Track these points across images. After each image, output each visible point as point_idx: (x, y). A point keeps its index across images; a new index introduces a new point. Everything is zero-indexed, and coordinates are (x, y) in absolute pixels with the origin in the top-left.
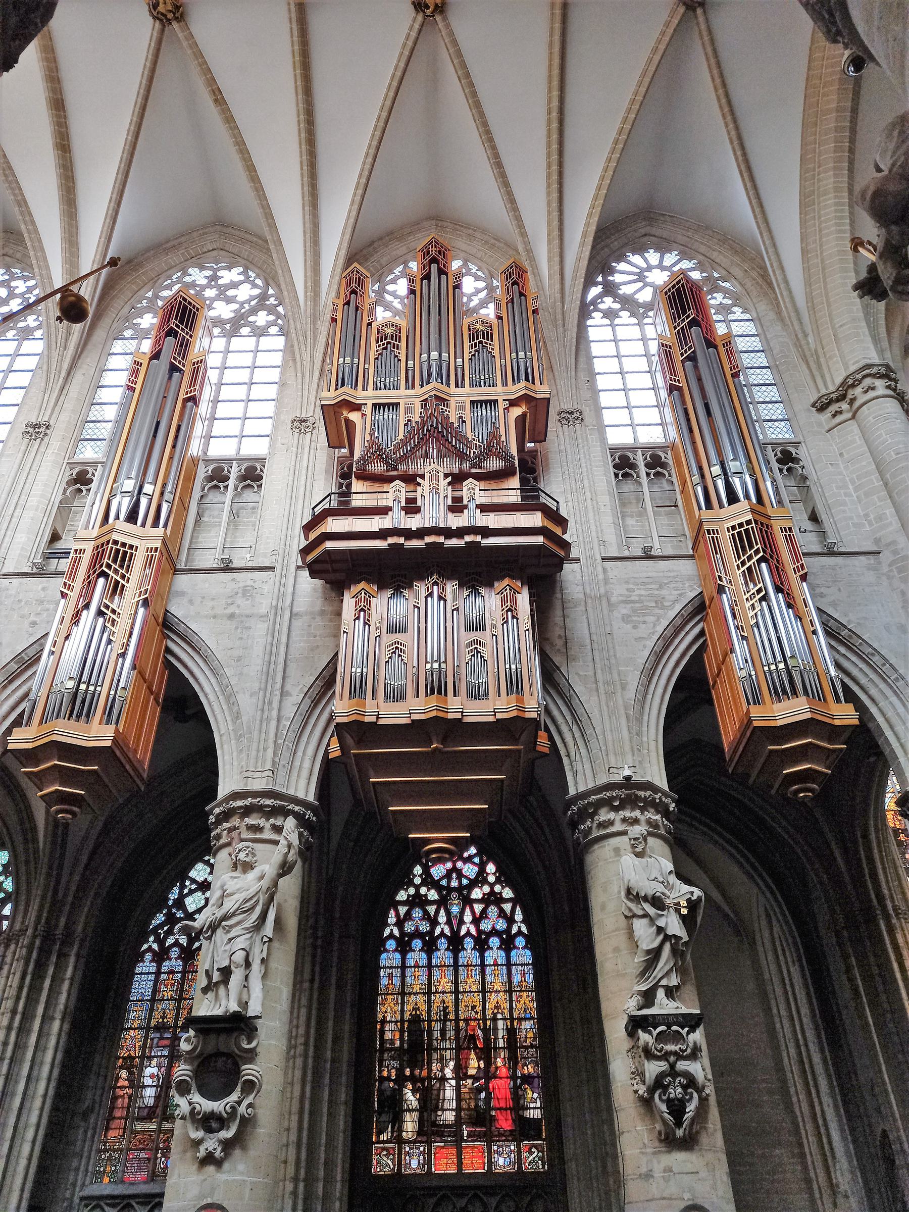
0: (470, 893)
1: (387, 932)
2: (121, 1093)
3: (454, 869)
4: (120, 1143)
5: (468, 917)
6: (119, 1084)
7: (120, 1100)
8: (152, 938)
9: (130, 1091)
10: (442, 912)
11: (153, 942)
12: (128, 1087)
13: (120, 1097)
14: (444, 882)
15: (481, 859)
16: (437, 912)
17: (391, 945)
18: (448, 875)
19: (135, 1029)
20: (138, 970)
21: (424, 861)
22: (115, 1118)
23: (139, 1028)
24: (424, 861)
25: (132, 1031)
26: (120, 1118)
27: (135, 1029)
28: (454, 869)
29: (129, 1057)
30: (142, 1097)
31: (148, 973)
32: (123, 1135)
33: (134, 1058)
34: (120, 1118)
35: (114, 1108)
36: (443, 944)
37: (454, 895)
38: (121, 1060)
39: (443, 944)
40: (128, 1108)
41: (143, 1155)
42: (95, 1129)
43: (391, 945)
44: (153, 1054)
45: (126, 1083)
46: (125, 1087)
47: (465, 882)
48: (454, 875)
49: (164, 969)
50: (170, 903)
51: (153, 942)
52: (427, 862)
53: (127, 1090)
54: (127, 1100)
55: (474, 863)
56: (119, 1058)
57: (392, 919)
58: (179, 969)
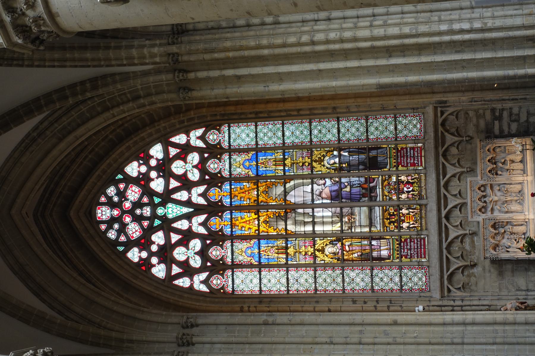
0: (157, 195)
1: (204, 288)
3: (131, 212)
5: (183, 196)
10: (177, 225)
14: (146, 223)
15: (120, 181)
16: (177, 231)
17: (216, 282)
18: (138, 219)
21: (121, 249)
24: (121, 249)
28: (131, 212)
36: (216, 223)
37: (160, 211)
39: (216, 223)
43: (216, 282)
47: (145, 200)
48: (138, 212)
52: (122, 244)
55: (126, 189)
57: (184, 282)
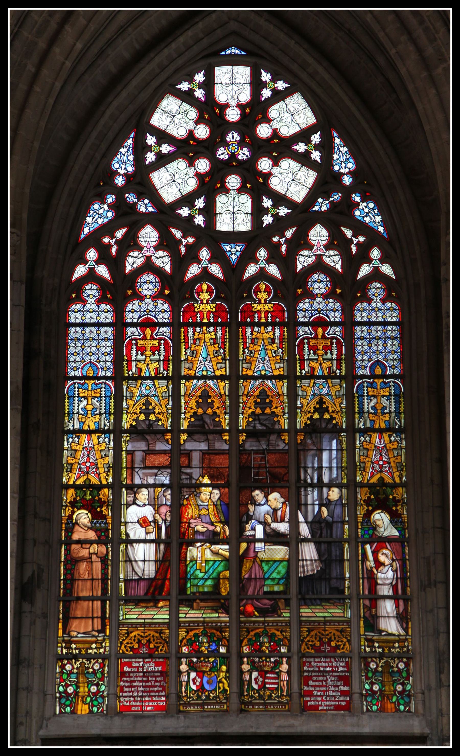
2: (84, 553)
4: (100, 644)
6: (76, 536)
7: (83, 566)
8: (92, 255)
9: (103, 549)
11: (98, 262)
12: (98, 542)
13: (82, 559)
19: (90, 432)
20: (74, 317)
22: (79, 599)
23: (100, 431)
25: (84, 437)
26: (92, 599)
27: (90, 432)
29: (88, 485)
30: (129, 560)
31: (98, 325)
32: (103, 630)
33: (100, 487)
34: (92, 599)
35: (73, 580)
38: (71, 491)
40: (104, 580)
41: (149, 666)
42: (45, 615)
44: (137, 481)
45: (92, 535)
46: (91, 542)
49: (130, 317)
50: (120, 181)
51: (98, 262)
53: (94, 548)
54: (97, 566)
56: (67, 487)
58: (165, 317)
